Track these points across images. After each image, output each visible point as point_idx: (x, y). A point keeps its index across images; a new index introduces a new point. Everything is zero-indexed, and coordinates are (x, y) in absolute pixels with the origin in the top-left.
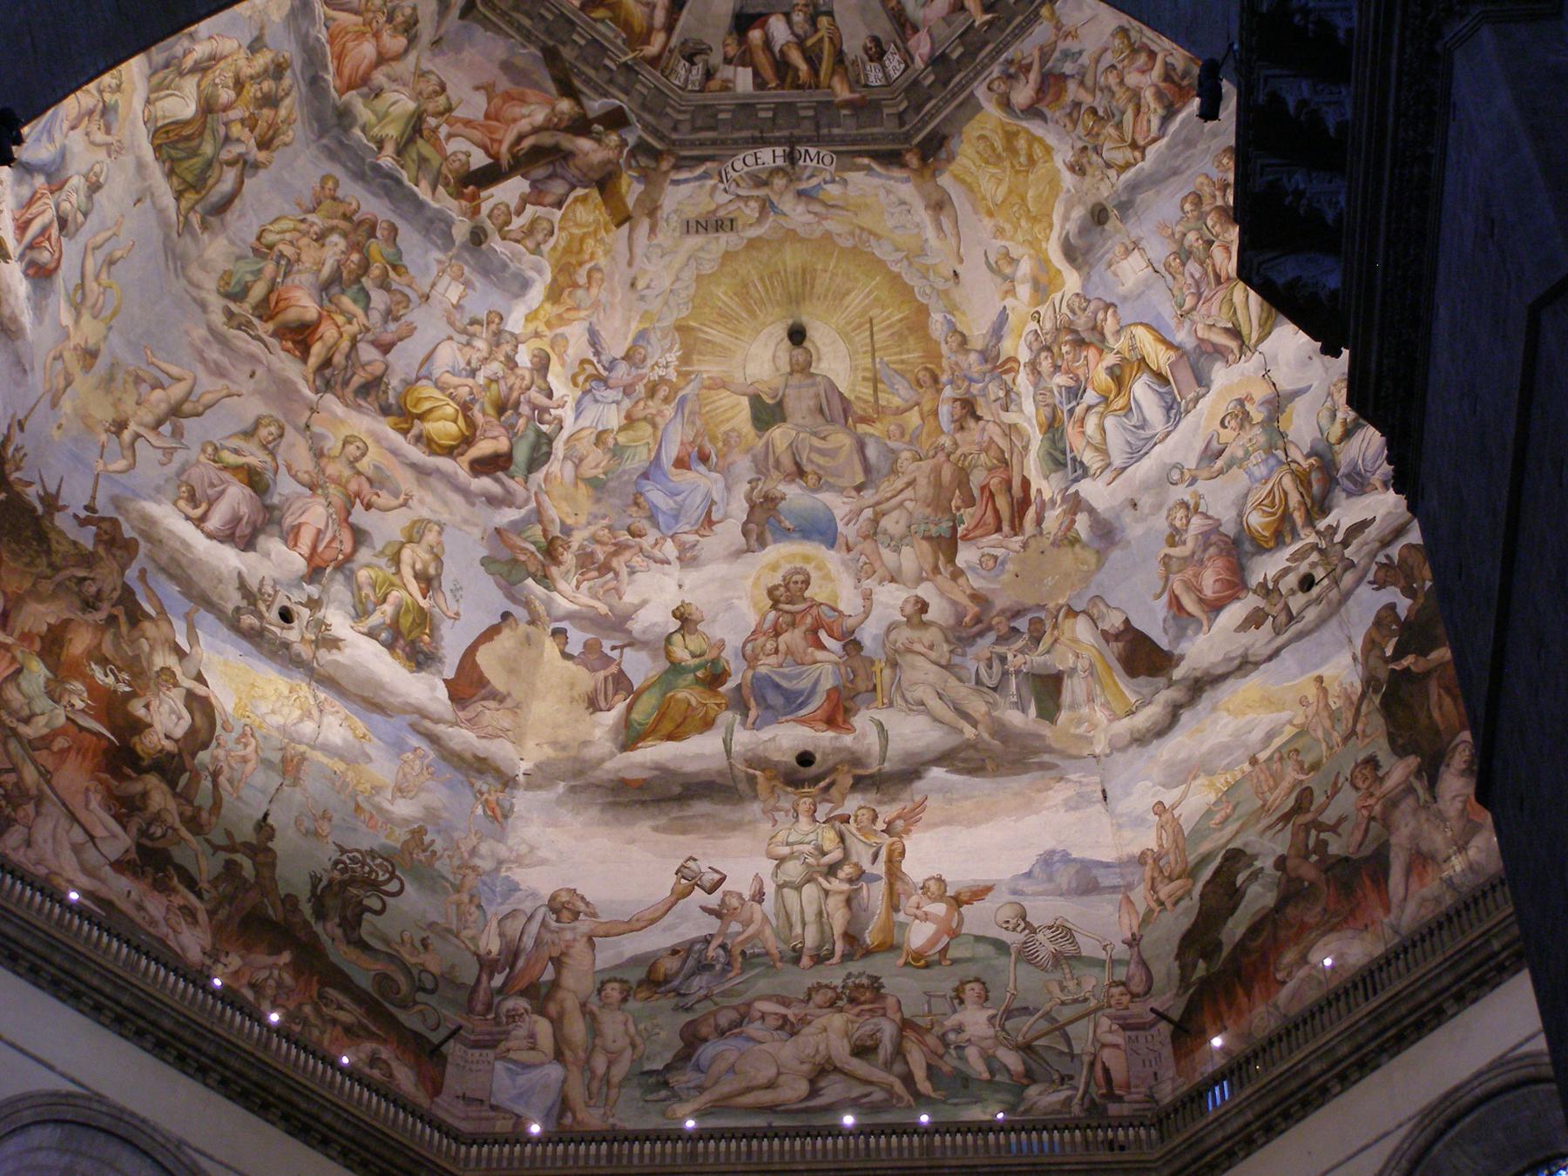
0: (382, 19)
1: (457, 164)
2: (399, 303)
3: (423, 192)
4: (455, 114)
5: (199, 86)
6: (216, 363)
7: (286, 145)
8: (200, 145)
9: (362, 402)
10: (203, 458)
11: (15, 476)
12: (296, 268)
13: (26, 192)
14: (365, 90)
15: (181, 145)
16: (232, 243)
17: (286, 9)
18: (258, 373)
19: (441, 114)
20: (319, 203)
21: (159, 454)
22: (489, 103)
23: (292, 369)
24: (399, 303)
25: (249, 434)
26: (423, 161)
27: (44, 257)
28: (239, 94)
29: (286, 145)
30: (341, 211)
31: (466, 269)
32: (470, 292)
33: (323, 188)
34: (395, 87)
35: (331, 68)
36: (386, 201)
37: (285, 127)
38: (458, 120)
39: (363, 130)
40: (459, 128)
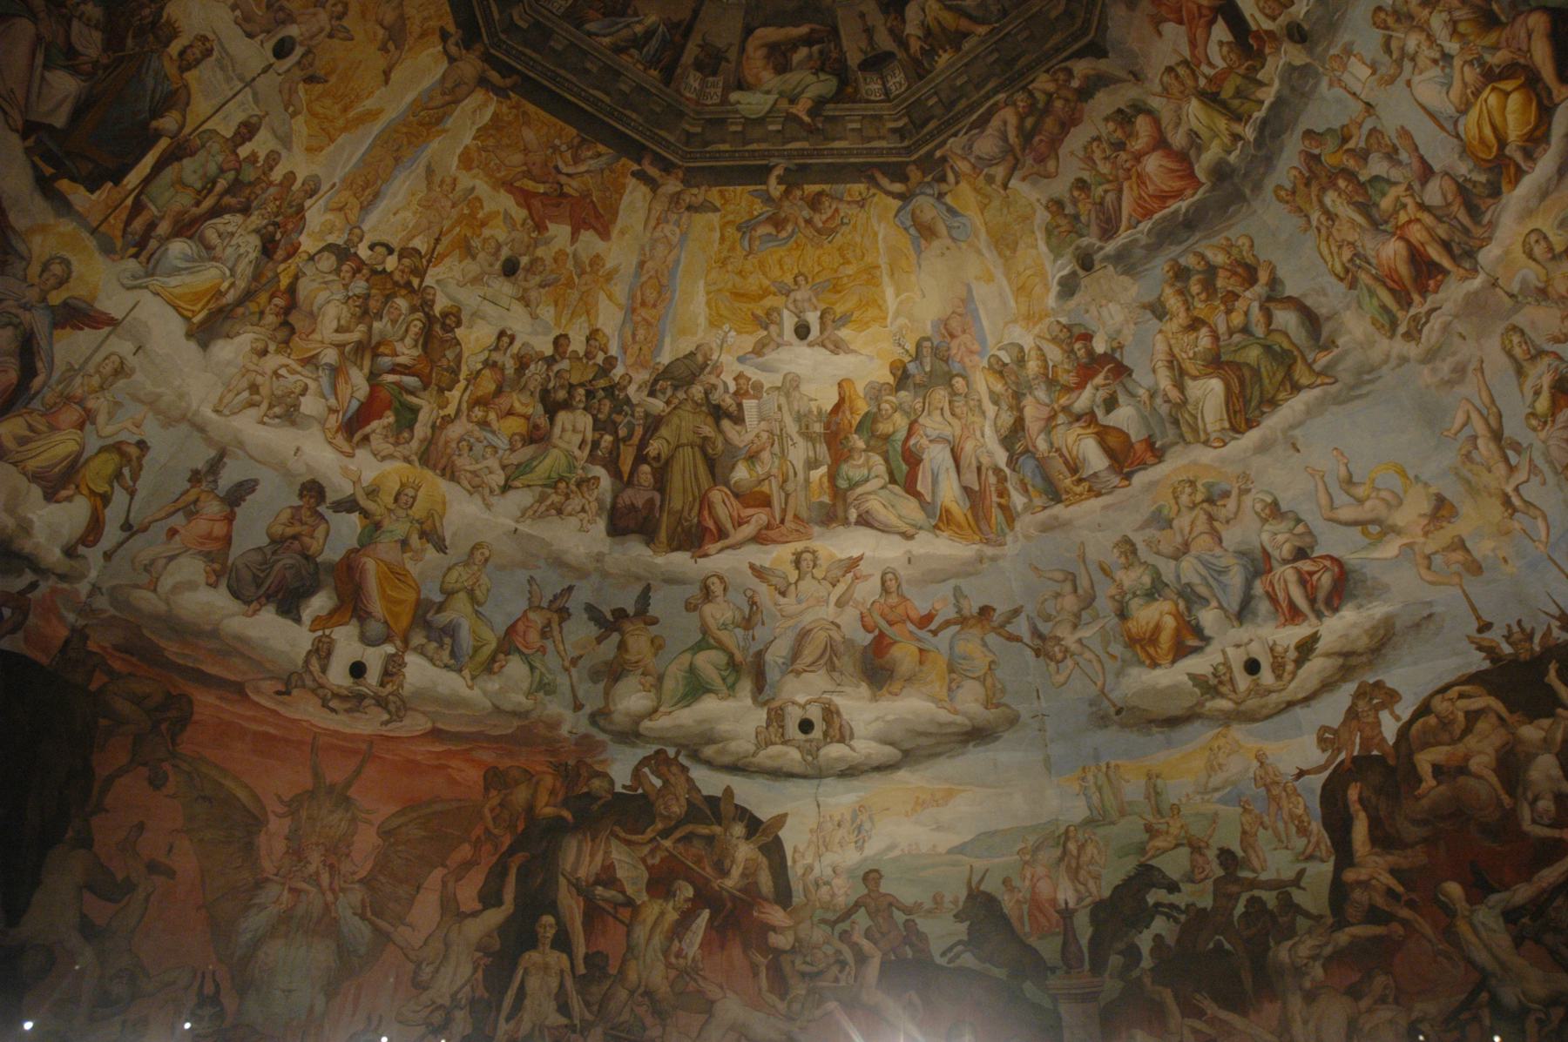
0: (1123, 156)
1: (1233, 56)
2: (1379, 143)
3: (1268, 95)
4: (1187, 54)
5: (1195, 378)
6: (1454, 370)
7: (1252, 246)
8: (1248, 364)
9: (1486, 219)
10: (1543, 435)
11: (1537, 649)
12: (1360, 249)
13: (1264, 607)
14: (1192, 153)
15: (1248, 391)
16: (1348, 307)
17: (1125, 279)
18: (1461, 329)
19: (1193, 72)
20: (1301, 210)
21: (1535, 480)
22: (1169, 20)
23: (1454, 291)
24: (1379, 143)
25: (1520, 372)
26: (1238, 93)
27: (1326, 580)
28: (1204, 323)
29: (1252, 246)
30: (1302, 187)
31: (1333, 52)
32: (1356, 49)
33: (1287, 202)
34: (1184, 118)
35: (1174, 206)
36: (1284, 137)
37: (1234, 251)
38: (1193, 55)
39: (1229, 153)
40: (1199, 51)
